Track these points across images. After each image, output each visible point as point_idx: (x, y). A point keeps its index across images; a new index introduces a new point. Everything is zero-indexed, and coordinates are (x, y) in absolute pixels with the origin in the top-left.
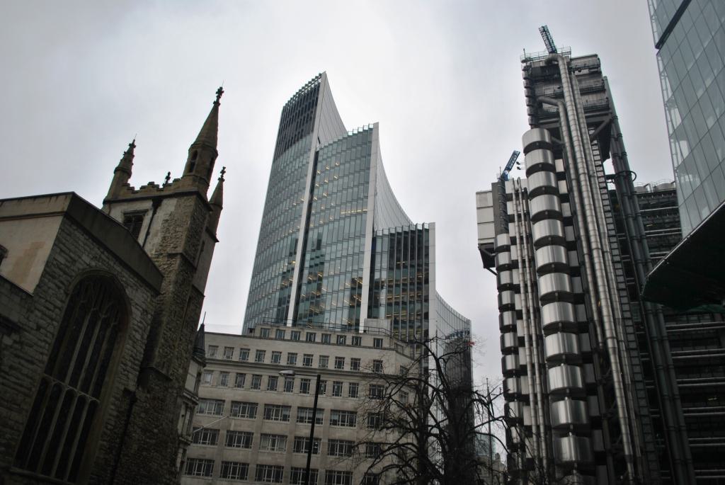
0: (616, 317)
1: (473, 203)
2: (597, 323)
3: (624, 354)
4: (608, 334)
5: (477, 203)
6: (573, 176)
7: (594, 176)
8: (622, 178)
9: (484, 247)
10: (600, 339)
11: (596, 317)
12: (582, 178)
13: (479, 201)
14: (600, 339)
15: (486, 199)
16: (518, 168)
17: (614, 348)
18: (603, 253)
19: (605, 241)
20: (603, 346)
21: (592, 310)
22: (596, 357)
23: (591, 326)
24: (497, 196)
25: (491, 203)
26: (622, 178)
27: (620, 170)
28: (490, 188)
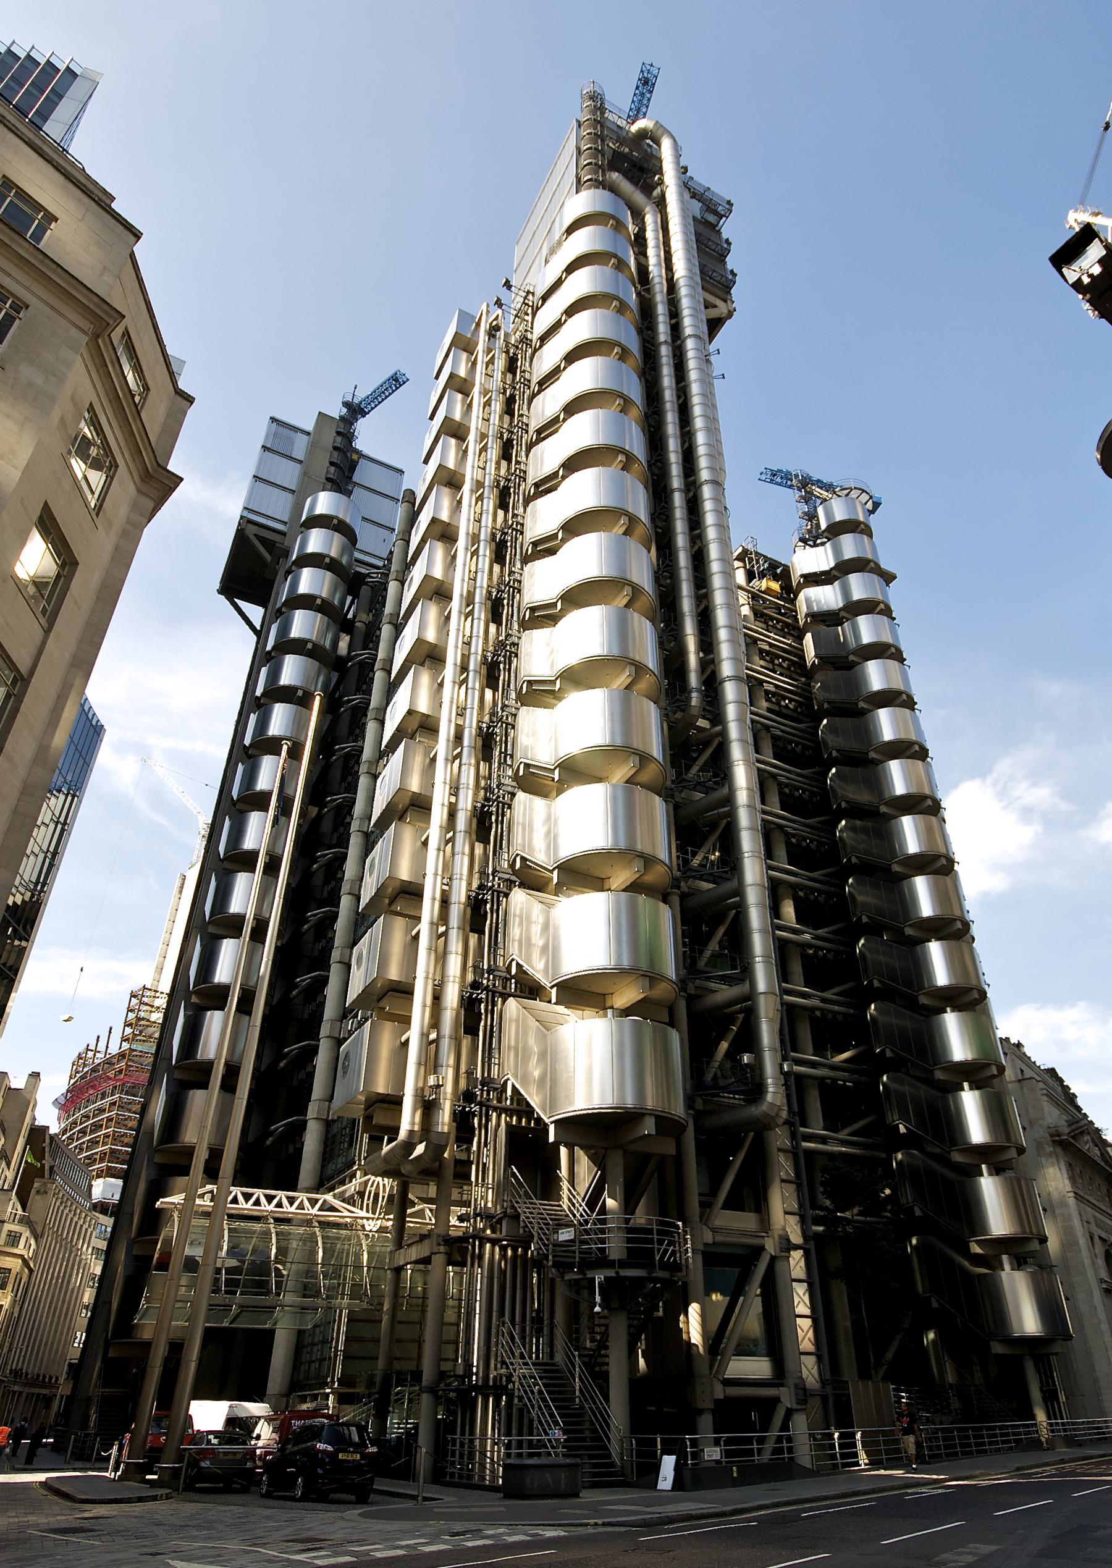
1: (259, 433)
5: (267, 437)
9: (250, 526)
13: (275, 435)
15: (291, 442)
16: (499, 303)
24: (329, 438)
25: (299, 452)
28: (309, 426)
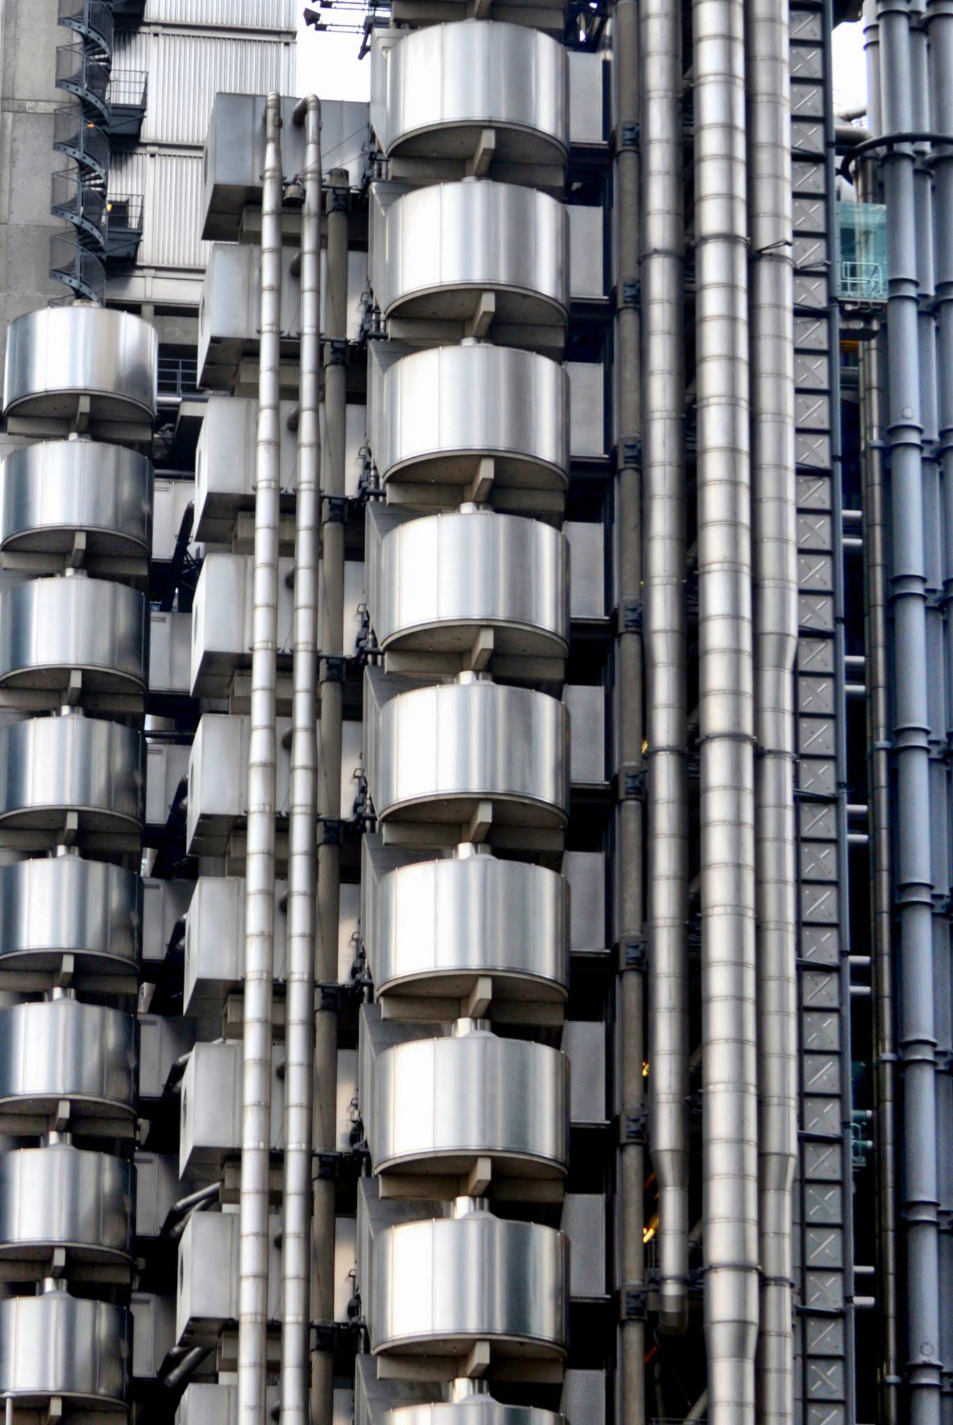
0: (773, 1145)
2: (669, 1169)
3: (783, 1353)
4: (720, 1246)
6: (659, 231)
7: (778, 258)
8: (907, 171)
10: (671, 1260)
11: (666, 1135)
12: (712, 262)
14: (671, 1260)
17: (741, 1324)
18: (759, 755)
19: (778, 686)
20: (681, 1299)
21: (648, 1085)
22: (632, 1338)
23: (631, 1159)
26: (907, 171)
27: (907, 128)
